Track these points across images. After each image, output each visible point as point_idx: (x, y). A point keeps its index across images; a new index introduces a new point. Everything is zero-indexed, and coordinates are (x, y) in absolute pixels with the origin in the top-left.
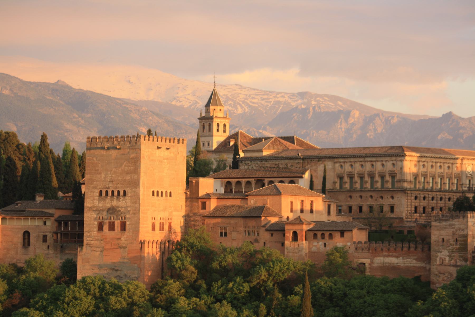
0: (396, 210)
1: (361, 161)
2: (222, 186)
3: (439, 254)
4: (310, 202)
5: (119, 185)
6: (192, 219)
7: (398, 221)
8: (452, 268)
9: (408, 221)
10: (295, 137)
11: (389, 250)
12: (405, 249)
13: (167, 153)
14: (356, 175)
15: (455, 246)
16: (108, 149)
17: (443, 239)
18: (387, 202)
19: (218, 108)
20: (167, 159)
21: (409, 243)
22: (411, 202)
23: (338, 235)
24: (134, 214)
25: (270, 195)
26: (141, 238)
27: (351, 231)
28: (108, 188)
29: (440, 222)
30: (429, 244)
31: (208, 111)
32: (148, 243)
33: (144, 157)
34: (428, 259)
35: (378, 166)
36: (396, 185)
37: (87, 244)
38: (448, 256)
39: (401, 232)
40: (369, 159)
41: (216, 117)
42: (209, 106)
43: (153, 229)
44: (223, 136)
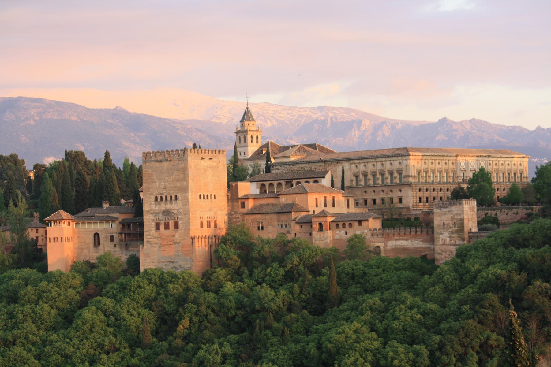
0: (403, 201)
1: (373, 162)
2: (257, 188)
3: (441, 236)
4: (331, 198)
5: (171, 191)
7: (406, 210)
8: (452, 247)
9: (414, 210)
10: (317, 144)
11: (399, 234)
12: (413, 233)
13: (210, 163)
14: (369, 174)
16: (161, 161)
17: (444, 223)
18: (396, 195)
19: (251, 123)
20: (210, 167)
21: (416, 228)
22: (416, 194)
23: (356, 224)
26: (192, 234)
27: (367, 220)
28: (162, 194)
29: (440, 209)
30: (433, 228)
31: (242, 126)
32: (198, 238)
33: (191, 167)
34: (432, 240)
35: (387, 165)
36: (403, 180)
37: (147, 242)
38: (449, 237)
39: (409, 219)
41: (250, 130)
42: (244, 122)
43: (202, 226)
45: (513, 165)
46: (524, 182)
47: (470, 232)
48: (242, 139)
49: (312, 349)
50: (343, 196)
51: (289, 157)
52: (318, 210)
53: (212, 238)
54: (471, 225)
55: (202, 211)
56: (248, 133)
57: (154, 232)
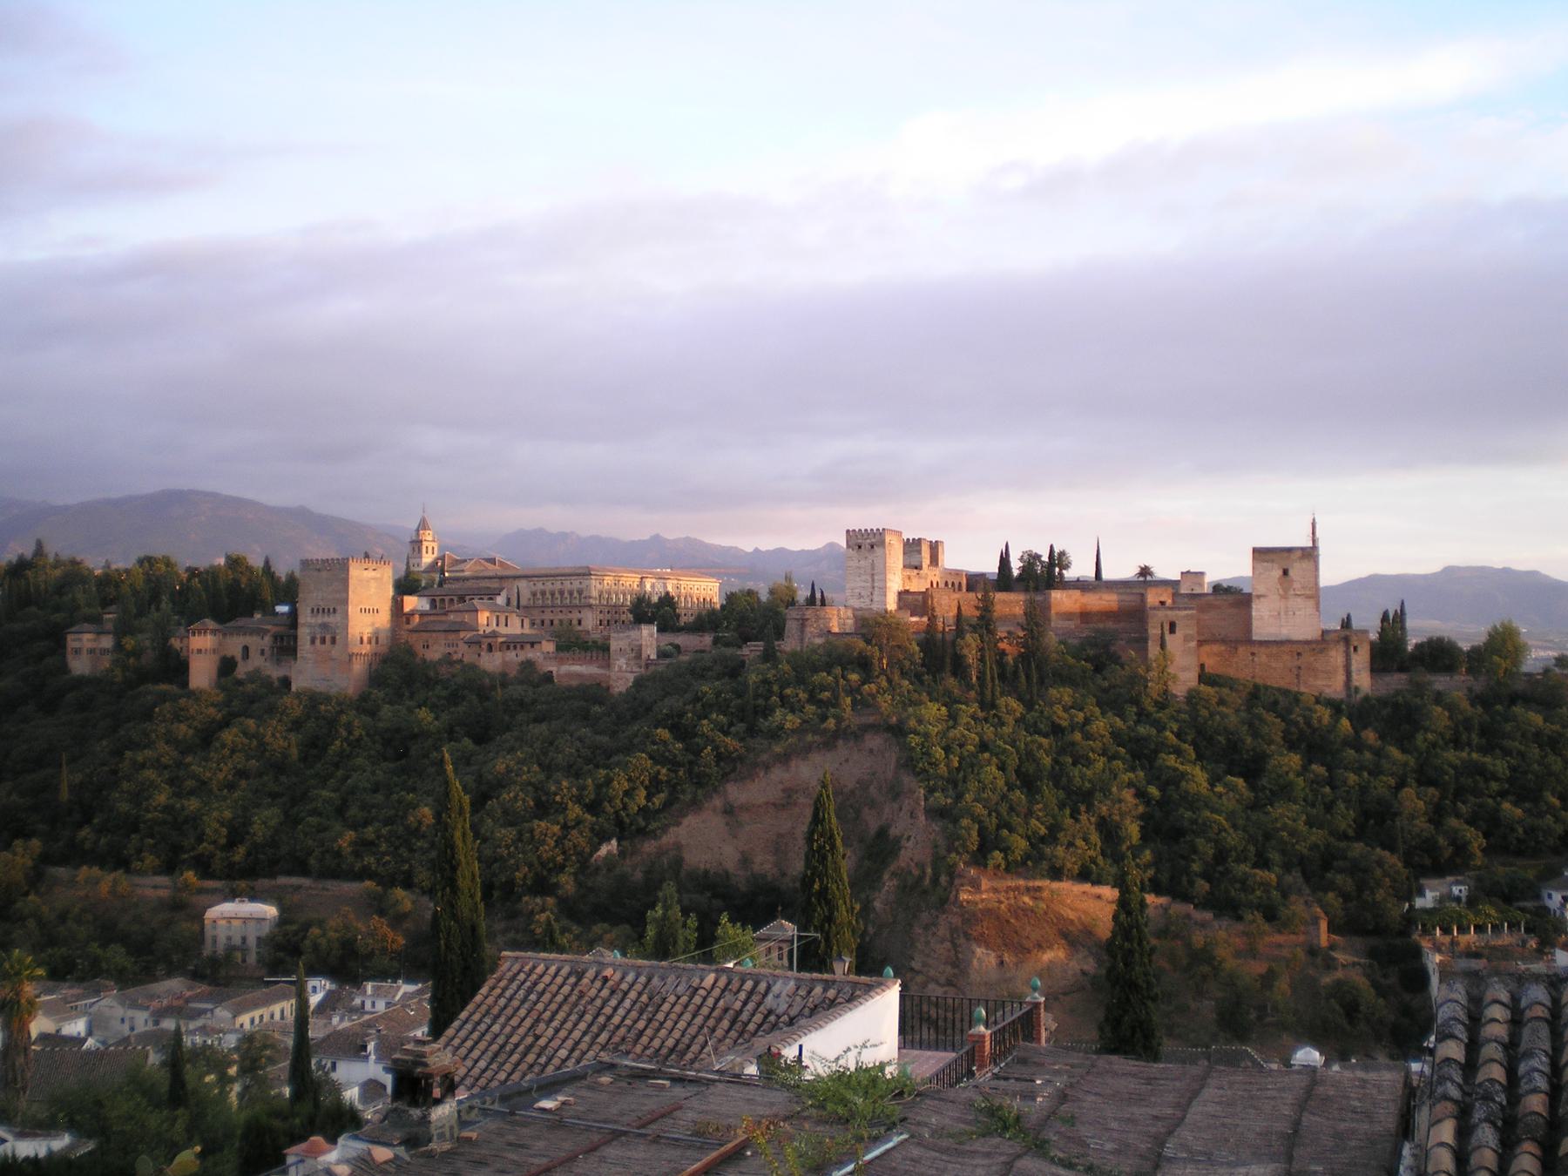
12: (588, 658)
13: (373, 574)
18: (575, 616)
23: (528, 646)
26: (350, 651)
34: (608, 666)
43: (362, 642)
51: (463, 571)
52: (488, 630)
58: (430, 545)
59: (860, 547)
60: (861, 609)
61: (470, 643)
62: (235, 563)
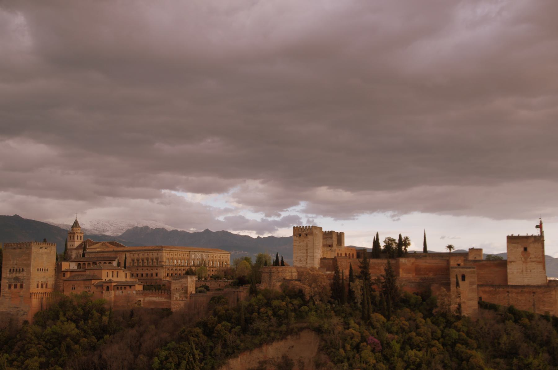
0: (158, 275)
1: (143, 253)
2: (76, 265)
3: (175, 295)
4: (116, 272)
5: (20, 266)
6: (58, 281)
7: (159, 280)
8: (180, 302)
9: (164, 280)
10: (115, 241)
11: (152, 294)
12: (160, 293)
13: (46, 250)
14: (140, 259)
15: (182, 292)
16: (15, 249)
17: (177, 288)
18: (154, 272)
19: (78, 228)
20: (46, 253)
21: (162, 290)
22: (166, 271)
23: (128, 287)
24: (27, 280)
25: (97, 269)
26: (31, 291)
27: (135, 285)
28: (15, 268)
29: (175, 281)
30: (170, 291)
31: (73, 230)
32: (39, 294)
33: (33, 252)
34: (170, 298)
35: (151, 255)
36: (159, 264)
37: (3, 295)
38: (179, 296)
39: (160, 285)
40: (146, 252)
41: (77, 233)
42: (73, 228)
43: (38, 287)
44: (80, 242)
45: (222, 258)
46: (227, 267)
47: (191, 294)
48: (72, 237)
49: (96, 359)
50: (123, 272)
51: (96, 248)
52: (107, 279)
53: (41, 294)
54: (192, 289)
55: (39, 278)
56: (76, 234)
57: (7, 290)
58: (79, 235)
59: (300, 235)
60: (301, 267)
61: (97, 286)
62: (512, 235)
